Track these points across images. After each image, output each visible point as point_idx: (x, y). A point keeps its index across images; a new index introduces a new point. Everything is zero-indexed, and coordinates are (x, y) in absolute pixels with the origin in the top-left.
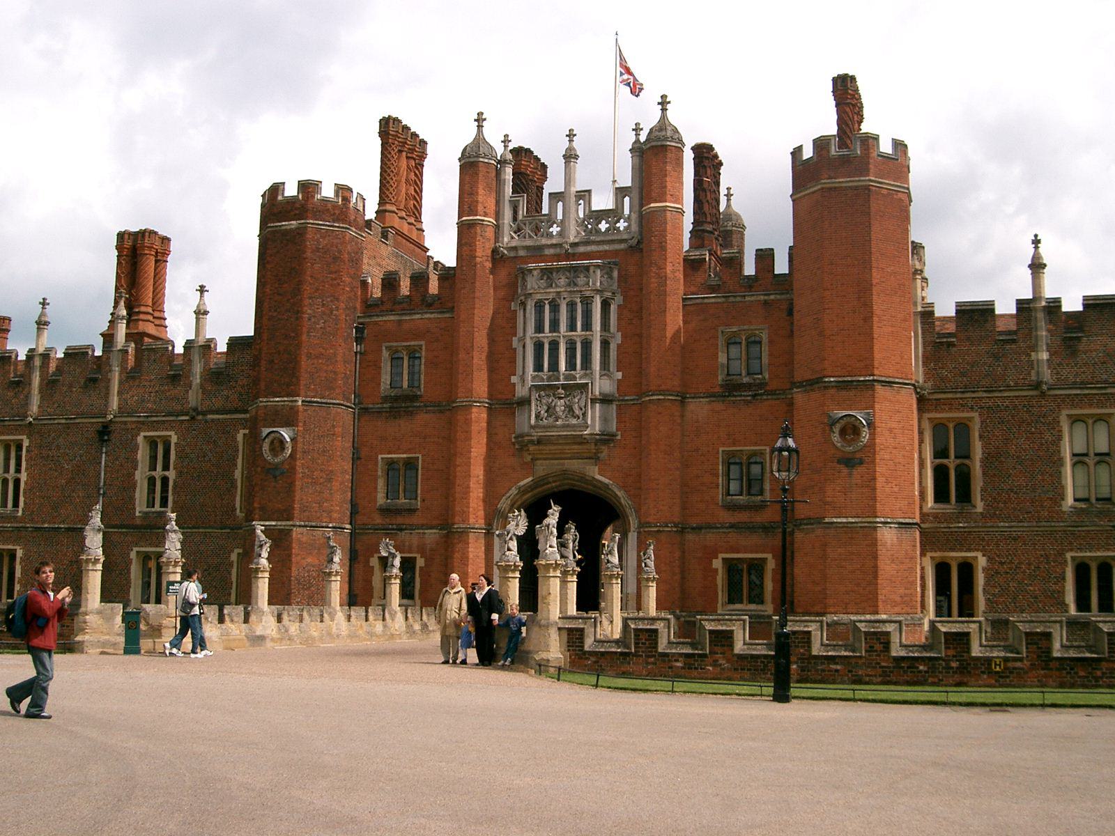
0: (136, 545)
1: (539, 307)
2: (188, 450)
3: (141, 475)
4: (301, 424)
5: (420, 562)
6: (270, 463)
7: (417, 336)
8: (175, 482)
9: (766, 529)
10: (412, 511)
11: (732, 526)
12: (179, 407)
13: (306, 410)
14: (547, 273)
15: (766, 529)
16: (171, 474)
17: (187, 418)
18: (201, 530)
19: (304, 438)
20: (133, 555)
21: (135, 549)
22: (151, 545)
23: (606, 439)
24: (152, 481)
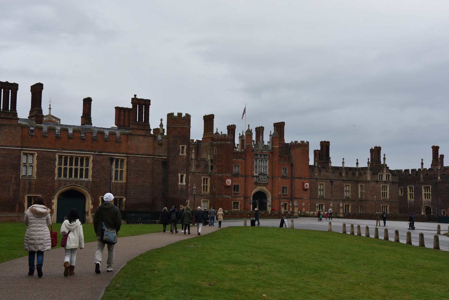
1: (259, 160)
5: (240, 203)
7: (238, 163)
9: (288, 199)
10: (238, 194)
11: (284, 198)
14: (261, 155)
15: (288, 199)
23: (268, 184)
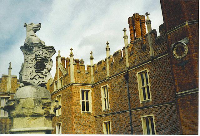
0: (142, 115)
2: (153, 74)
3: (140, 88)
4: (190, 34)
6: (178, 60)
8: (151, 87)
12: (147, 59)
13: (192, 27)
16: (149, 85)
17: (150, 61)
18: (164, 105)
19: (194, 41)
20: (142, 119)
21: (142, 116)
22: (147, 114)
24: (144, 89)
